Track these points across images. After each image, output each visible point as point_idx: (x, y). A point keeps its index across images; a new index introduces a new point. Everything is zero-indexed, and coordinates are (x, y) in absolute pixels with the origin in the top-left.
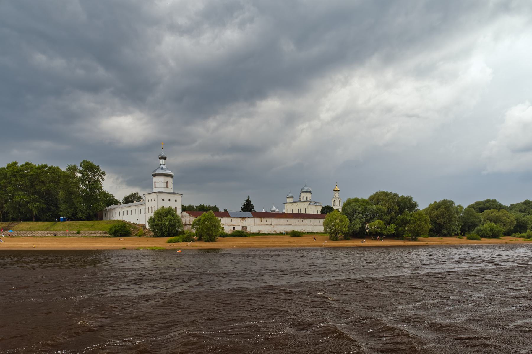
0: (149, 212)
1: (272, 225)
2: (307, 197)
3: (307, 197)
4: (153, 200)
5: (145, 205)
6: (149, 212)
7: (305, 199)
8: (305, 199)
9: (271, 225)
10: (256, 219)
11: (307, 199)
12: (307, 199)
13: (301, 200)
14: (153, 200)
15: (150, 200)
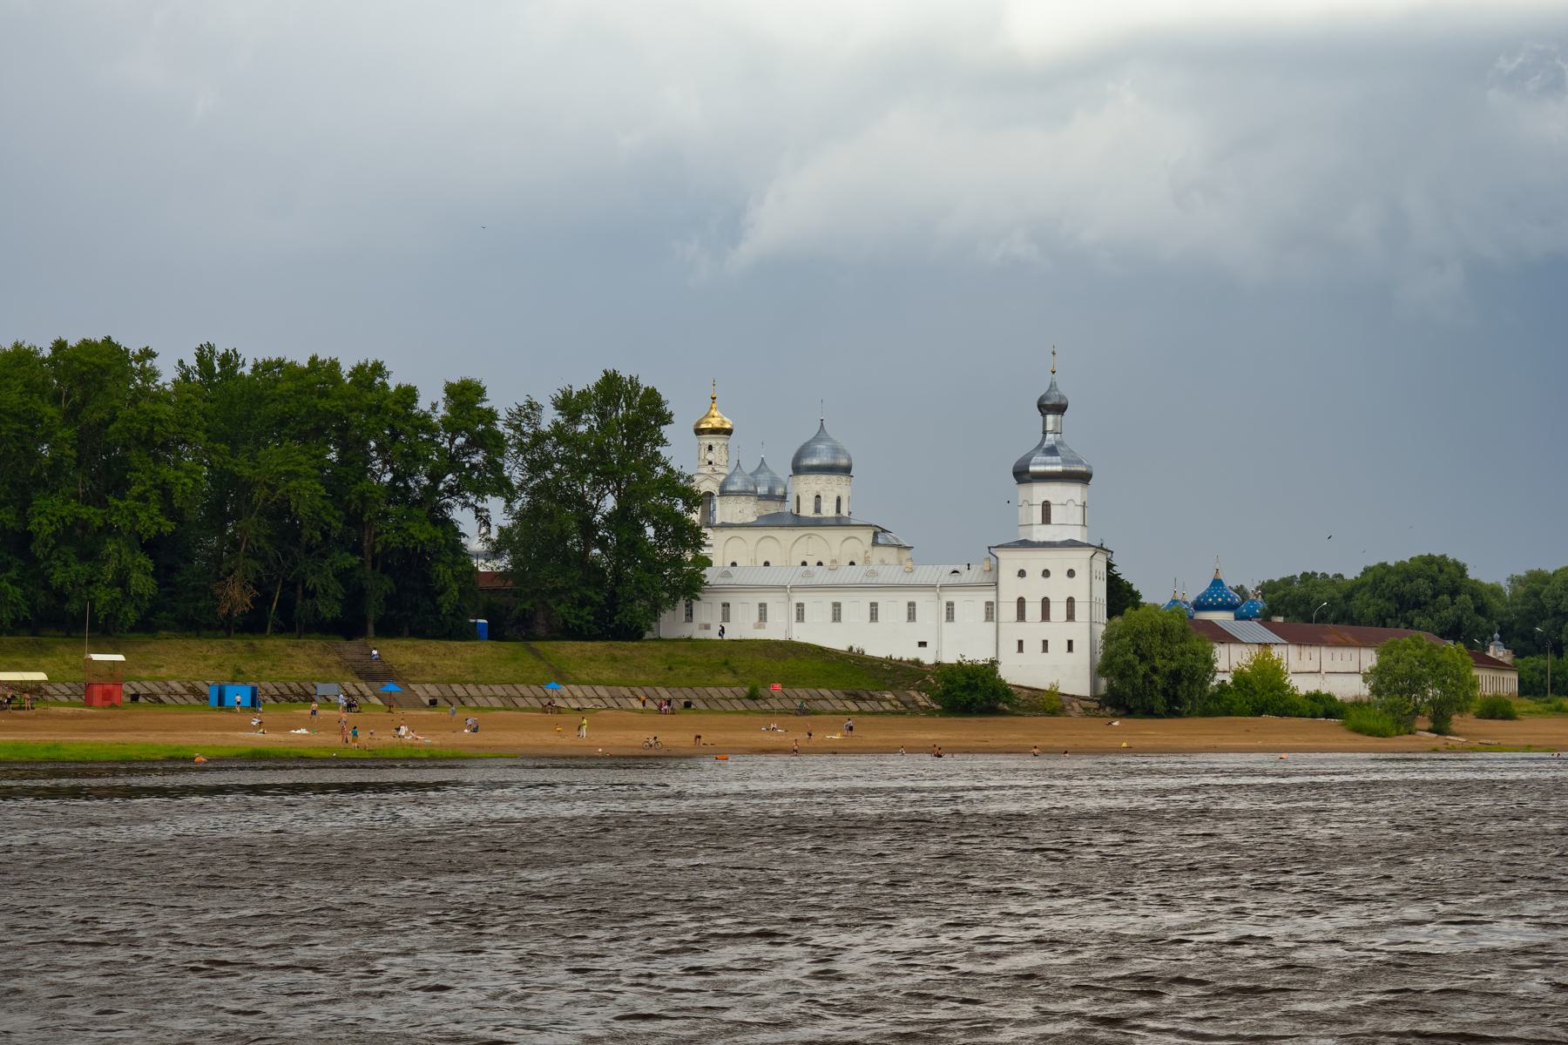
0: (1021, 616)
1: (1323, 672)
2: (839, 500)
3: (839, 500)
4: (1059, 575)
5: (997, 590)
6: (1021, 616)
7: (828, 510)
8: (828, 510)
9: (1320, 672)
10: (1290, 647)
11: (838, 511)
12: (838, 511)
13: (807, 510)
14: (1059, 575)
15: (1034, 572)
